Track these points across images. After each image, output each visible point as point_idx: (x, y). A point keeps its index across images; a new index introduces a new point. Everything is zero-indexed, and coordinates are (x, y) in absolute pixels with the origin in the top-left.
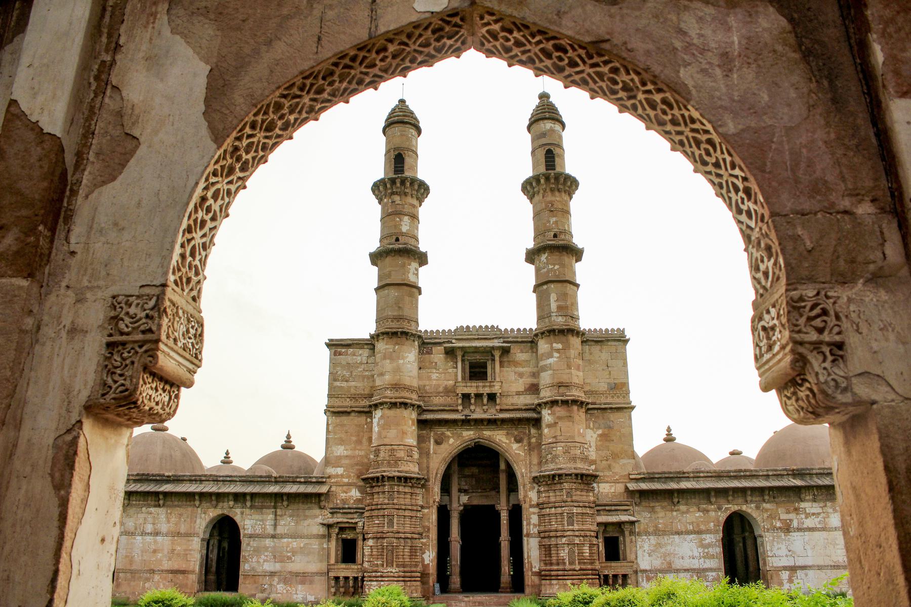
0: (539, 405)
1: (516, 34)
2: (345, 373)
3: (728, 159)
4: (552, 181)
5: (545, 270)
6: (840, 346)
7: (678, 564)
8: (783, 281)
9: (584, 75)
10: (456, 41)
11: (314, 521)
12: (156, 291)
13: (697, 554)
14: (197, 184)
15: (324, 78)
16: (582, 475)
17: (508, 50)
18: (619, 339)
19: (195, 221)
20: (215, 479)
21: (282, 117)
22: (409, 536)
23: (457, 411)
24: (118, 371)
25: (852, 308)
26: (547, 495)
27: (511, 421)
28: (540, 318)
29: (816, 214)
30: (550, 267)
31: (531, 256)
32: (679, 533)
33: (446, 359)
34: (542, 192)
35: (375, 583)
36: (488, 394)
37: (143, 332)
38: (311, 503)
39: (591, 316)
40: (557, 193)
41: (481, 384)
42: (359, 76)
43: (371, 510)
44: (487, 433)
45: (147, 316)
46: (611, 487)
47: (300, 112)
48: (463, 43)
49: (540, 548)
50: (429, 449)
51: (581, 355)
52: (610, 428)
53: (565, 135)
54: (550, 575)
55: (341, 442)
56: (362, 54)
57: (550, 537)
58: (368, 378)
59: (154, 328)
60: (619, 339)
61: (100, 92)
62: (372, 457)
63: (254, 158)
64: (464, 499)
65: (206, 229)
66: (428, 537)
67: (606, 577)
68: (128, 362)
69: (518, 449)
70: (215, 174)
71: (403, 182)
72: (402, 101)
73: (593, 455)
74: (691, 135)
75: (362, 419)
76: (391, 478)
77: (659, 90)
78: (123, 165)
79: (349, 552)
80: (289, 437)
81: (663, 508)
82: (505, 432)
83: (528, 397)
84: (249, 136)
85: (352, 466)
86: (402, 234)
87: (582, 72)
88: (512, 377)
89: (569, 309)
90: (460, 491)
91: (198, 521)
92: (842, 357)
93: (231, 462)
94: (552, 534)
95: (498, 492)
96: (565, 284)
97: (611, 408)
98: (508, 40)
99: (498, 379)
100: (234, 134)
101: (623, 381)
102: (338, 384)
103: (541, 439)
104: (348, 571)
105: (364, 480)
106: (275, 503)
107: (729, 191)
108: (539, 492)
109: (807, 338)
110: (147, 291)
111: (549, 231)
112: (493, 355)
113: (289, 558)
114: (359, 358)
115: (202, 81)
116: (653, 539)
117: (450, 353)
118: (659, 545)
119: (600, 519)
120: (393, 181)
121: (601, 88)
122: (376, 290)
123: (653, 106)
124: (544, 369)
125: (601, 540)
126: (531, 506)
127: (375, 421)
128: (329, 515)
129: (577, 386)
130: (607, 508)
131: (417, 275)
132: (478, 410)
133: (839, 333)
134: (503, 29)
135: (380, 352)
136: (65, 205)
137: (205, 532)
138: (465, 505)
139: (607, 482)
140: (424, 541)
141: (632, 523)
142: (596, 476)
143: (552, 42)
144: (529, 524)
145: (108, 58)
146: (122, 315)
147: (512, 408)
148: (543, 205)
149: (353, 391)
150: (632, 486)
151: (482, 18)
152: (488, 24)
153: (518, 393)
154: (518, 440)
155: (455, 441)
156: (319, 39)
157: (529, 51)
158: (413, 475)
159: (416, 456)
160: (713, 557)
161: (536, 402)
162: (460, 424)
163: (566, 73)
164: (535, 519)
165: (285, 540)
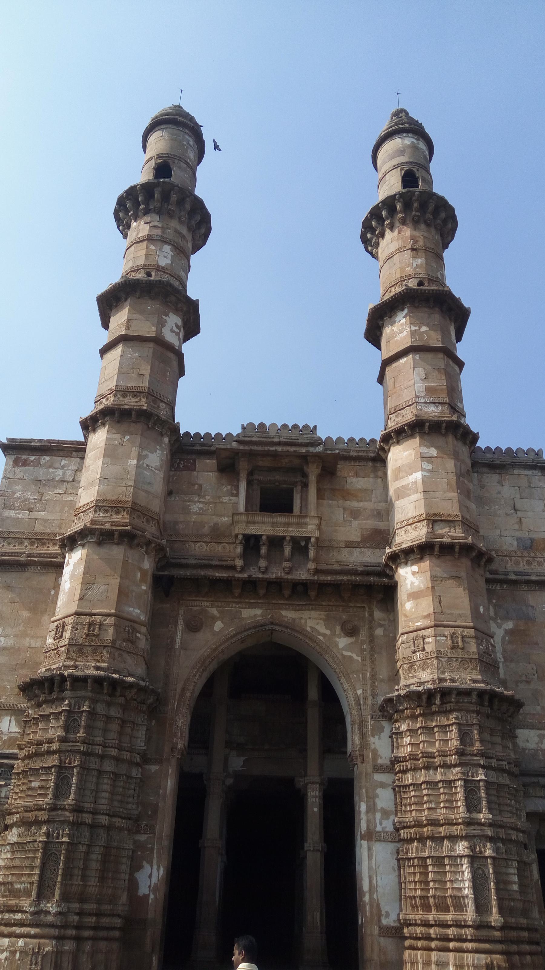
2: (28, 495)
4: (416, 205)
5: (405, 333)
22: (104, 820)
23: (233, 568)
30: (413, 328)
36: (295, 540)
40: (423, 226)
41: (279, 520)
44: (288, 615)
50: (173, 639)
54: (429, 938)
62: (50, 641)
66: (151, 829)
69: (349, 647)
71: (165, 197)
76: (79, 681)
82: (323, 614)
86: (159, 269)
88: (339, 515)
96: (441, 355)
97: (529, 582)
99: (313, 513)
102: (12, 513)
112: (305, 475)
114: (60, 472)
120: (147, 189)
124: (402, 493)
125: (534, 856)
126: (378, 769)
127: (67, 570)
135: (94, 448)
139: (532, 727)
140: (142, 838)
144: (372, 809)
147: (337, 567)
148: (400, 241)
149: (39, 528)
153: (350, 545)
154: (351, 631)
155: (222, 627)
159: (143, 643)
164: (385, 798)
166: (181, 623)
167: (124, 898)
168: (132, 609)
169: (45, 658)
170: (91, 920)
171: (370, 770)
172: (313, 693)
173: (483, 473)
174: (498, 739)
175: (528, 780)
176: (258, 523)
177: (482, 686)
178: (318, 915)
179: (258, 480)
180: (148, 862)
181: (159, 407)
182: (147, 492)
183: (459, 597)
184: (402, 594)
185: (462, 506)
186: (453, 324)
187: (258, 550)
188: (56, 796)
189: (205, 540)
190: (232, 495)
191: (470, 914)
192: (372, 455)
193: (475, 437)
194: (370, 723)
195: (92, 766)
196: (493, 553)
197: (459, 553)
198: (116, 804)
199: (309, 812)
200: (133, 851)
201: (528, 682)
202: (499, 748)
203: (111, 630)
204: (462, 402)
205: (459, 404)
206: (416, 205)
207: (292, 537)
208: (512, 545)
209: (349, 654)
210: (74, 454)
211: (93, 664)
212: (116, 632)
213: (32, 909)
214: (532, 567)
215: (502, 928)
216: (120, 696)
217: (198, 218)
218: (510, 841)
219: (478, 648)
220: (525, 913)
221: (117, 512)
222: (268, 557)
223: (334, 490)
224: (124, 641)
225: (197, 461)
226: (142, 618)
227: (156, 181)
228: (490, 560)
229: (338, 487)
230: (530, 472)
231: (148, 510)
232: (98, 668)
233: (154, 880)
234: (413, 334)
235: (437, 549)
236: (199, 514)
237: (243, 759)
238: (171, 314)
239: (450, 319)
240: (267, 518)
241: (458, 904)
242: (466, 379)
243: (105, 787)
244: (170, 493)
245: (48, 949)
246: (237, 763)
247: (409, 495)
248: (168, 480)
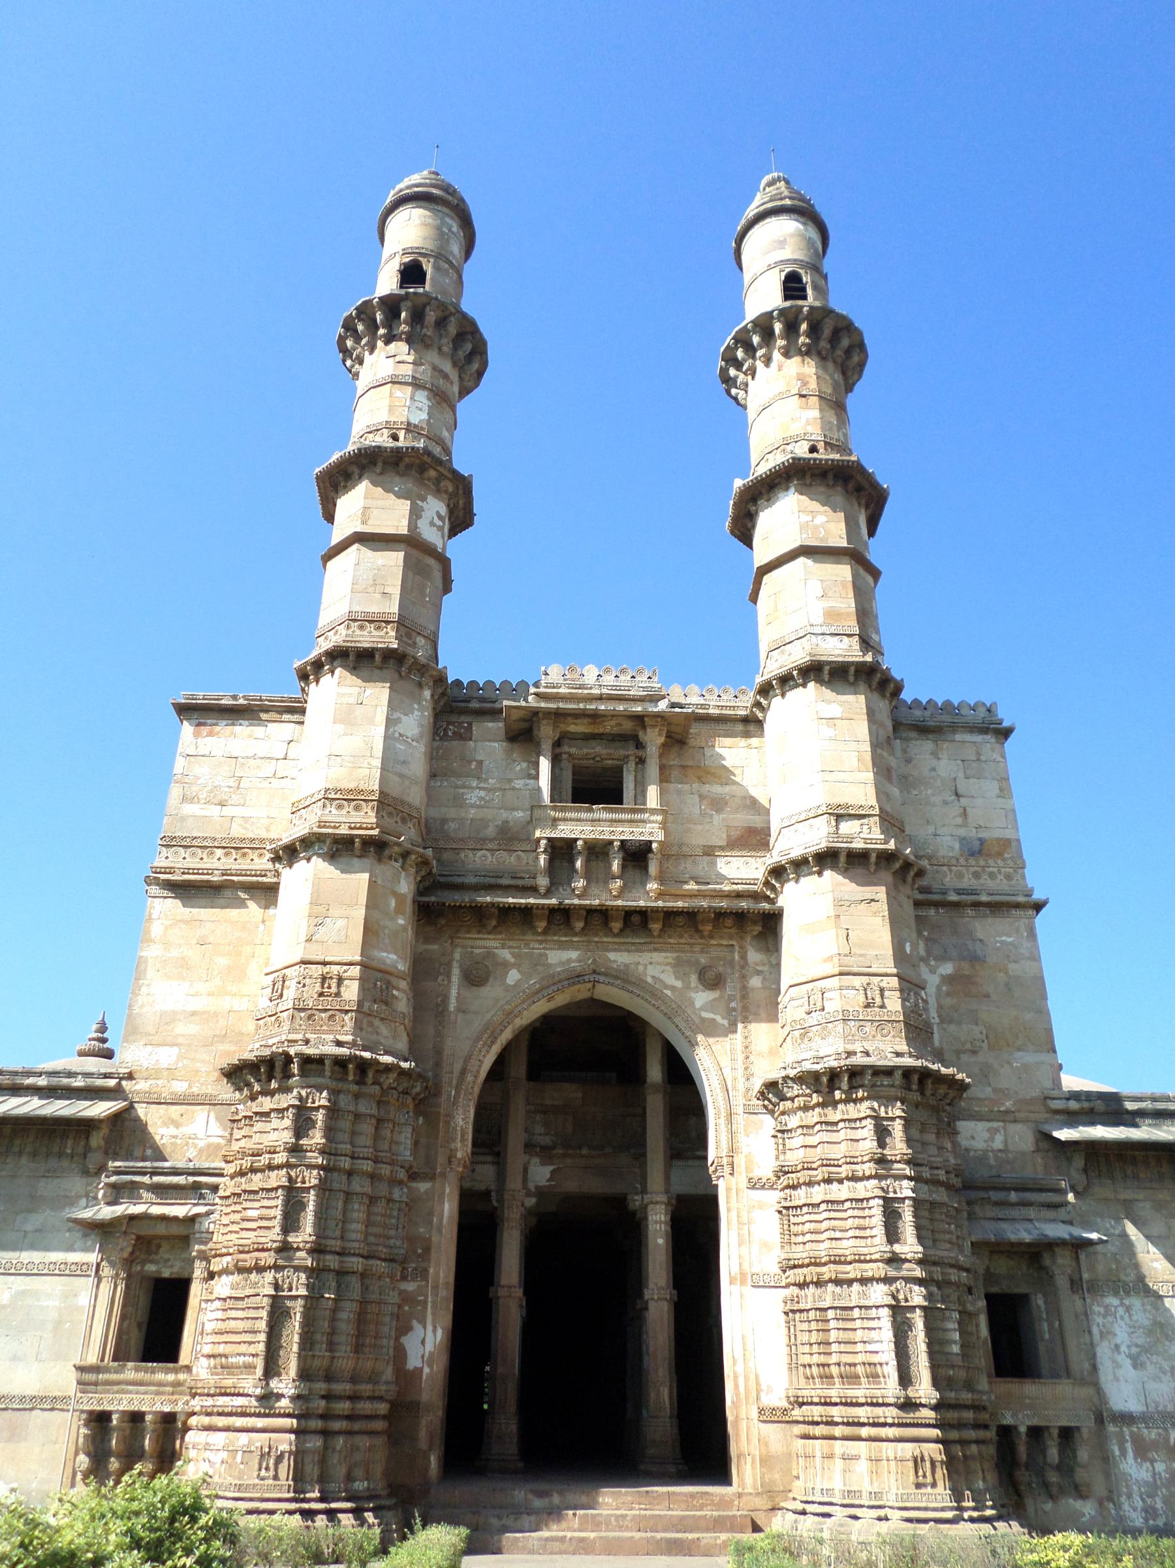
0: (778, 872)
22: (356, 1263)
33: (508, 753)
35: (219, 1438)
38: (61, 1155)
43: (242, 1174)
44: (618, 958)
46: (993, 1132)
50: (446, 998)
52: (975, 959)
64: (541, 1174)
66: (423, 1274)
67: (1006, 1433)
71: (417, 317)
79: (155, 1326)
80: (103, 1028)
81: (1159, 1206)
82: (670, 956)
85: (208, 1044)
90: (529, 1147)
95: (640, 1156)
97: (976, 905)
101: (1008, 834)
104: (142, 1392)
112: (640, 745)
120: (391, 305)
125: (982, 1303)
126: (754, 1184)
130: (995, 1196)
138: (540, 1193)
139: (979, 1117)
140: (410, 1286)
149: (237, 831)
154: (713, 982)
159: (403, 1004)
162: (541, 925)
166: (456, 973)
167: (389, 1374)
168: (385, 954)
169: (258, 1028)
170: (344, 1406)
171: (744, 1183)
172: (655, 1072)
173: (907, 739)
174: (931, 1137)
175: (973, 1195)
176: (571, 820)
177: (908, 1061)
178: (665, 1392)
179: (570, 755)
180: (419, 1322)
181: (415, 643)
182: (401, 775)
184: (789, 928)
185: (881, 793)
186: (863, 511)
187: (572, 862)
189: (490, 846)
190: (530, 777)
191: (891, 1388)
192: (743, 713)
193: (899, 688)
194: (740, 1120)
195: (336, 1186)
196: (925, 863)
197: (877, 864)
198: (372, 1239)
199: (651, 1246)
200: (399, 1307)
201: (974, 1052)
202: (933, 1150)
203: (355, 985)
204: (878, 632)
205: (874, 636)
207: (622, 841)
208: (952, 848)
209: (712, 1016)
210: (286, 717)
211: (331, 1037)
212: (362, 988)
213: (258, 1391)
214: (982, 881)
216: (373, 1084)
217: (469, 347)
218: (949, 1283)
219: (903, 1006)
221: (357, 808)
222: (588, 875)
223: (683, 767)
224: (375, 1001)
225: (474, 724)
226: (401, 967)
227: (403, 292)
228: (921, 873)
229: (690, 763)
230: (978, 738)
231: (403, 803)
232: (339, 1044)
233: (429, 1347)
234: (804, 527)
235: (843, 859)
236: (479, 807)
237: (551, 1168)
238: (430, 498)
239: (859, 504)
240: (583, 813)
242: (883, 594)
243: (355, 1215)
244: (433, 775)
245: (284, 1447)
246: (541, 1174)
248: (433, 756)
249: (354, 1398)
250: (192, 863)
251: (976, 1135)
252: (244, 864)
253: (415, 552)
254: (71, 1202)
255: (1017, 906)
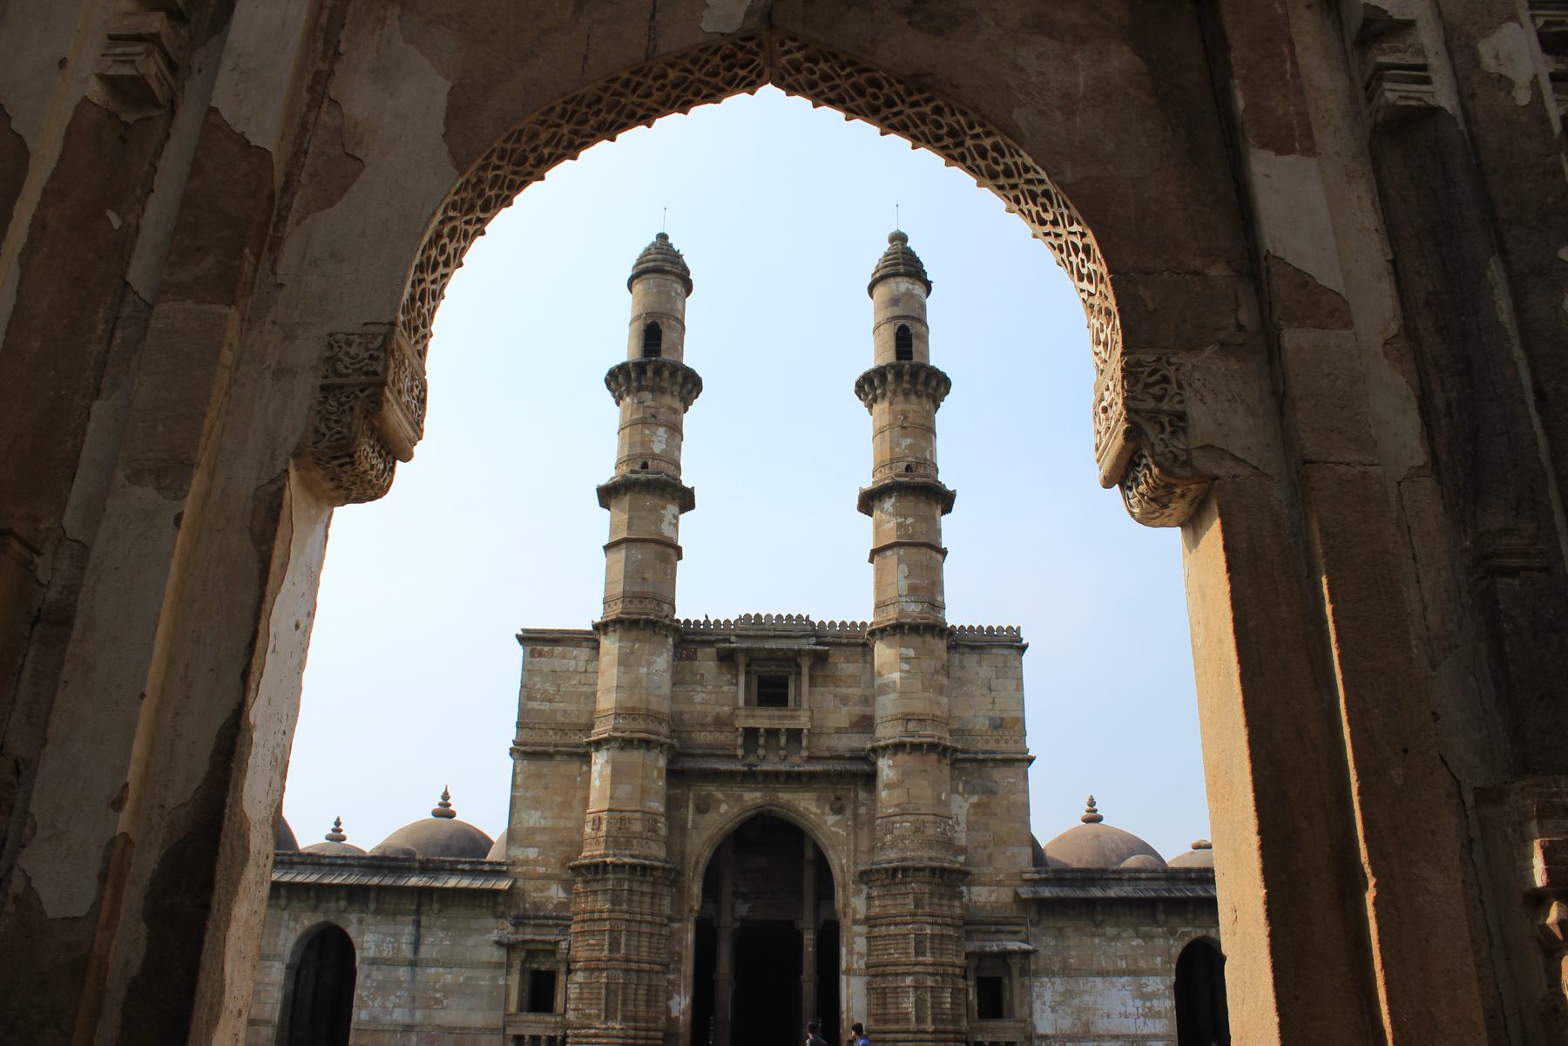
0: (874, 750)
1: (822, 65)
2: (547, 686)
3: (1066, 212)
4: (906, 378)
6: (1182, 416)
7: (1101, 1026)
8: (1120, 345)
9: (903, 117)
10: (751, 72)
11: (484, 941)
12: (384, 329)
13: (1133, 1010)
14: (434, 213)
15: (589, 106)
16: (943, 870)
17: (813, 85)
18: (1010, 644)
19: (428, 258)
20: (313, 860)
21: (534, 150)
22: (646, 966)
23: (735, 756)
24: (334, 417)
25: (1196, 376)
26: (884, 902)
27: (826, 776)
28: (880, 606)
29: (1161, 273)
31: (868, 502)
32: (1103, 974)
34: (889, 395)
36: (788, 730)
37: (367, 373)
39: (964, 607)
40: (913, 398)
42: (630, 106)
43: (584, 921)
44: (784, 797)
45: (371, 357)
46: (991, 892)
47: (557, 146)
48: (760, 75)
49: (868, 994)
51: (946, 669)
52: (991, 792)
53: (929, 302)
55: (536, 804)
56: (636, 79)
57: (884, 975)
58: (587, 697)
59: (380, 369)
60: (1010, 644)
61: (315, 105)
63: (497, 197)
64: (743, 909)
65: (437, 275)
66: (678, 970)
68: (346, 407)
69: (836, 824)
70: (454, 206)
71: (658, 371)
72: (663, 237)
73: (962, 838)
74: (1026, 187)
75: (574, 767)
76: (617, 867)
77: (989, 134)
78: (344, 189)
79: (540, 993)
80: (446, 796)
82: (813, 795)
83: (856, 737)
84: (497, 168)
86: (654, 457)
87: (901, 112)
88: (830, 702)
89: (929, 589)
90: (735, 894)
91: (283, 933)
92: (1183, 429)
93: (344, 838)
94: (888, 969)
96: (923, 550)
97: (994, 760)
98: (812, 72)
99: (805, 706)
100: (479, 162)
102: (534, 705)
103: (875, 809)
105: (574, 868)
106: (419, 906)
107: (1069, 255)
108: (869, 898)
109: (1141, 405)
110: (372, 329)
111: (899, 460)
112: (798, 666)
113: (438, 1001)
114: (573, 663)
115: (441, 100)
116: (1059, 984)
117: (727, 658)
118: (1069, 994)
119: (972, 947)
120: (640, 367)
121: (923, 133)
122: (607, 548)
123: (984, 157)
125: (971, 983)
126: (856, 922)
127: (595, 769)
128: (510, 929)
129: (935, 720)
130: (983, 928)
131: (676, 526)
132: (771, 756)
133: (1181, 402)
134: (808, 59)
136: (271, 232)
137: (293, 953)
139: (984, 884)
140: (672, 977)
141: (1026, 954)
142: (967, 874)
143: (865, 75)
144: (850, 952)
145: (324, 67)
146: (341, 355)
147: (826, 754)
149: (559, 718)
150: (1025, 892)
151: (782, 45)
152: (789, 52)
153: (839, 731)
154: (838, 811)
155: (728, 808)
156: (586, 58)
157: (838, 86)
158: (656, 863)
159: (663, 831)
160: (1158, 1015)
161: (869, 746)
163: (882, 115)
164: (861, 945)
165: (433, 970)
174: (946, 902)
183: (923, 790)
188: (610, 951)
191: (912, 1025)
194: (852, 887)
204: (942, 593)
206: (906, 378)
215: (934, 1032)
220: (955, 1021)
222: (766, 747)
230: (1006, 652)
232: (632, 856)
234: (899, 526)
241: (902, 1017)
246: (743, 909)
247: (886, 693)
249: (648, 1030)
250: (536, 739)
251: (981, 895)
252: (566, 741)
253: (660, 548)
254: (490, 931)
255: (1018, 760)
